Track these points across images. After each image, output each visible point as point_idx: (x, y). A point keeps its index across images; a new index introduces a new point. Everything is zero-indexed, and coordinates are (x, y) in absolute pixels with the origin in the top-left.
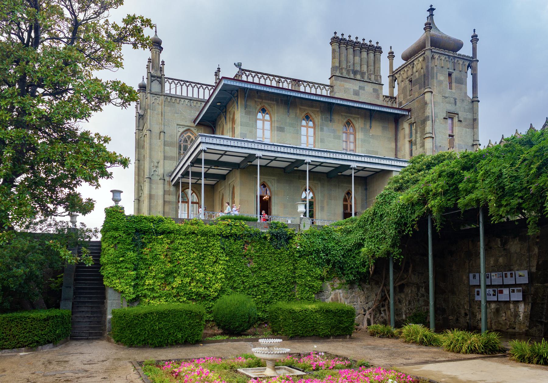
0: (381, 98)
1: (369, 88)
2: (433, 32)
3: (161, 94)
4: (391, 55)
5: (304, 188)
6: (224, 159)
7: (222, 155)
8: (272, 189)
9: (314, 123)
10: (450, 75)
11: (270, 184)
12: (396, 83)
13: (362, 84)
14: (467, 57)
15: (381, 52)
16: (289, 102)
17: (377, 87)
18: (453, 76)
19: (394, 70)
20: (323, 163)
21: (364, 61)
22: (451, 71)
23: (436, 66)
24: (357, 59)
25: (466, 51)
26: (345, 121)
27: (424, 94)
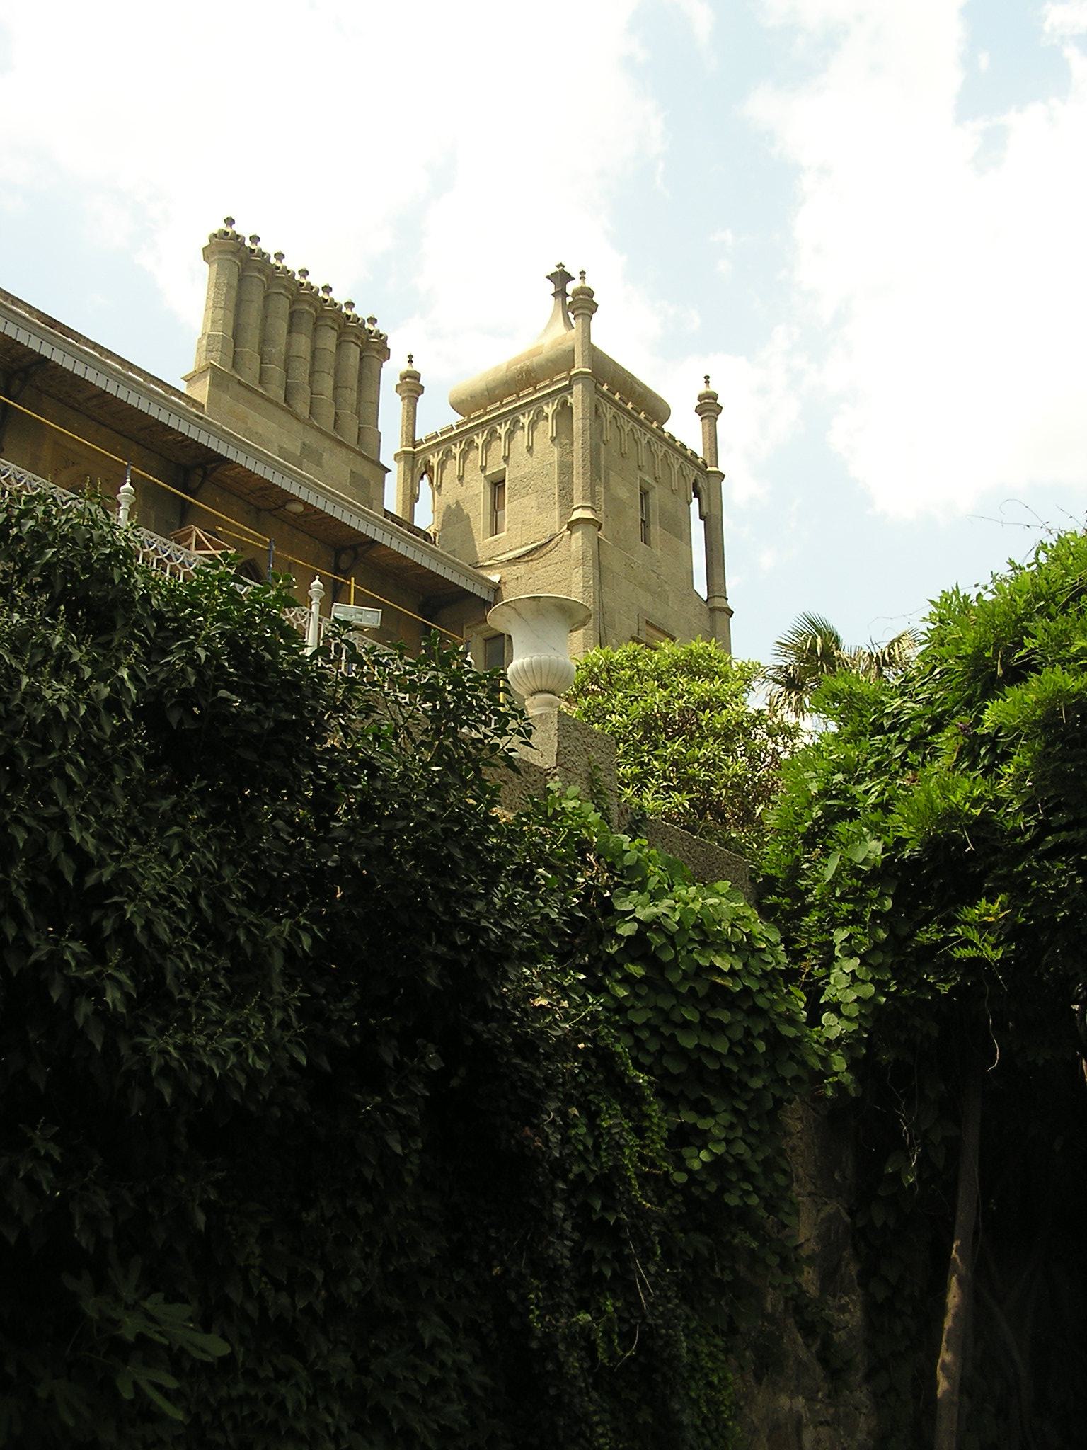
1: (338, 464)
10: (644, 494)
13: (312, 439)
15: (385, 353)
17: (365, 470)
18: (655, 497)
21: (328, 361)
22: (646, 478)
24: (302, 344)
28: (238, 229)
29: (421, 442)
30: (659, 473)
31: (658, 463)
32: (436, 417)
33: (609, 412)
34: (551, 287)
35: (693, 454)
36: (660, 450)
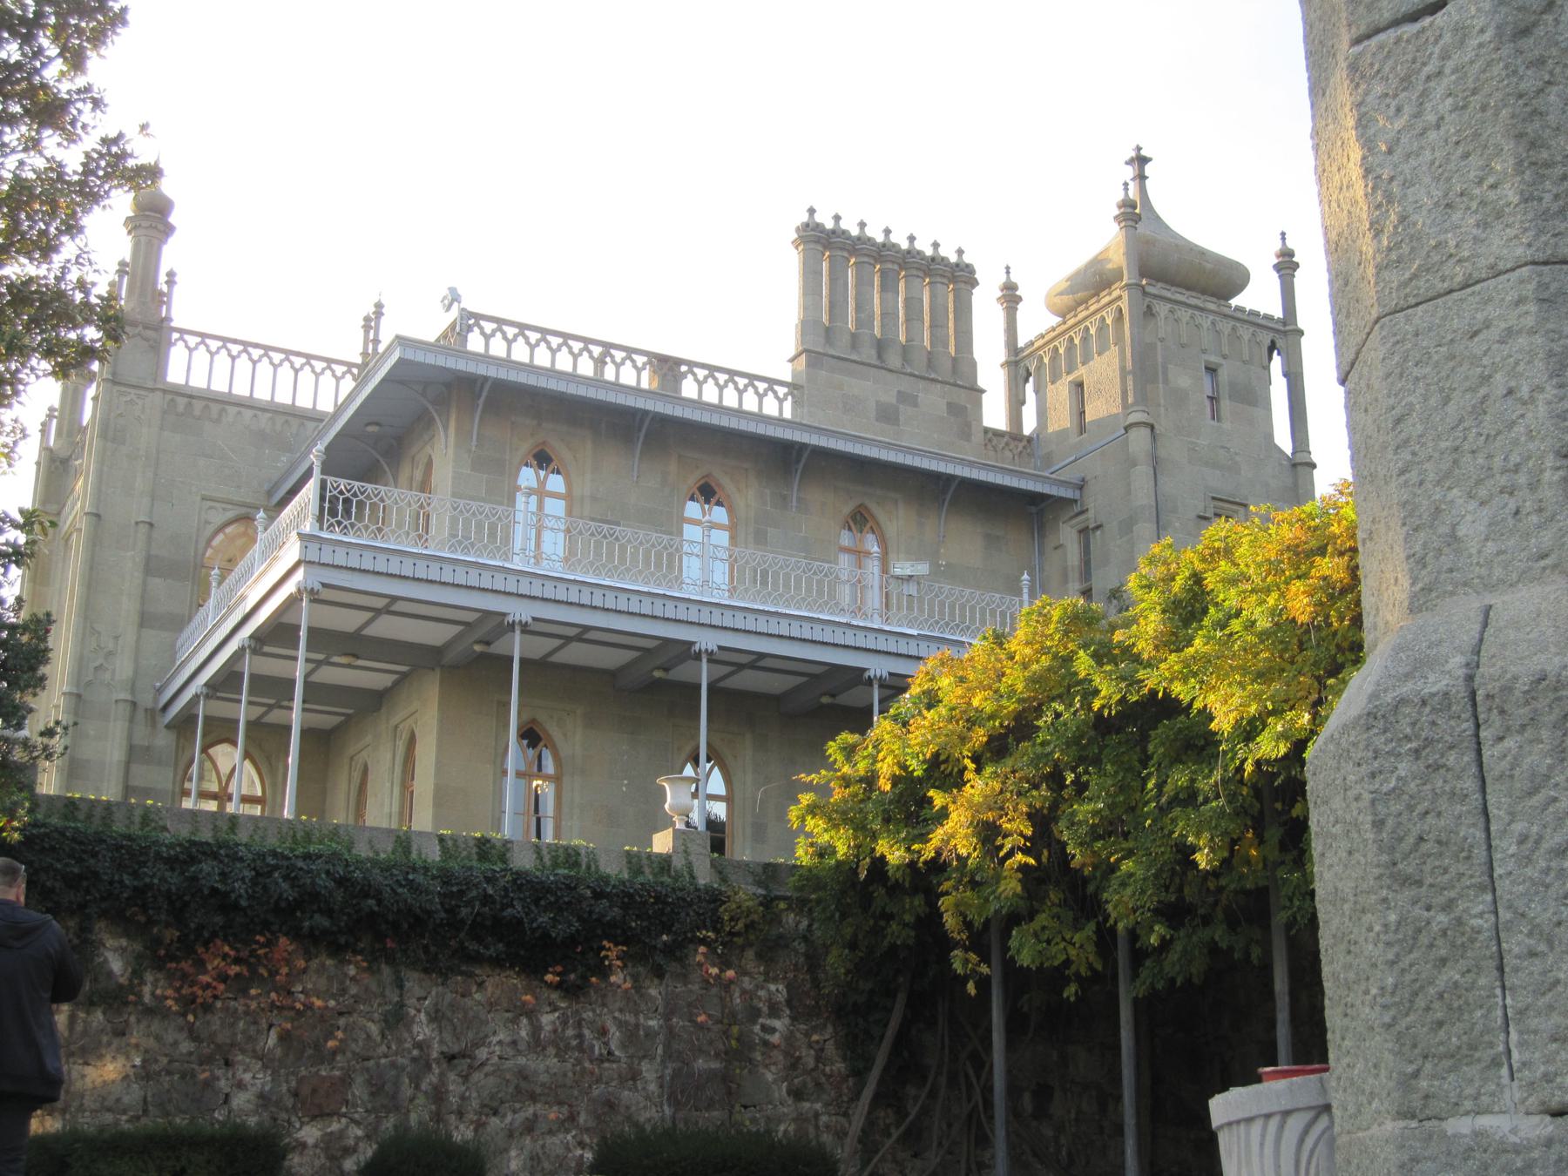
0: (978, 438)
1: (933, 400)
2: (1142, 228)
3: (150, 385)
4: (1010, 297)
5: (688, 749)
6: (386, 628)
7: (378, 612)
8: (565, 750)
9: (731, 511)
11: (555, 732)
12: (1030, 387)
13: (906, 384)
14: (1267, 317)
15: (974, 283)
16: (643, 437)
17: (962, 397)
18: (1224, 375)
19: (1021, 344)
20: (762, 656)
22: (1213, 359)
23: (1162, 340)
25: (1260, 297)
26: (847, 509)
27: (1127, 429)
28: (818, 218)
29: (1022, 350)
30: (1226, 350)
31: (1225, 340)
32: (1035, 321)
33: (1162, 309)
34: (1129, 172)
35: (1268, 317)
36: (1226, 327)
